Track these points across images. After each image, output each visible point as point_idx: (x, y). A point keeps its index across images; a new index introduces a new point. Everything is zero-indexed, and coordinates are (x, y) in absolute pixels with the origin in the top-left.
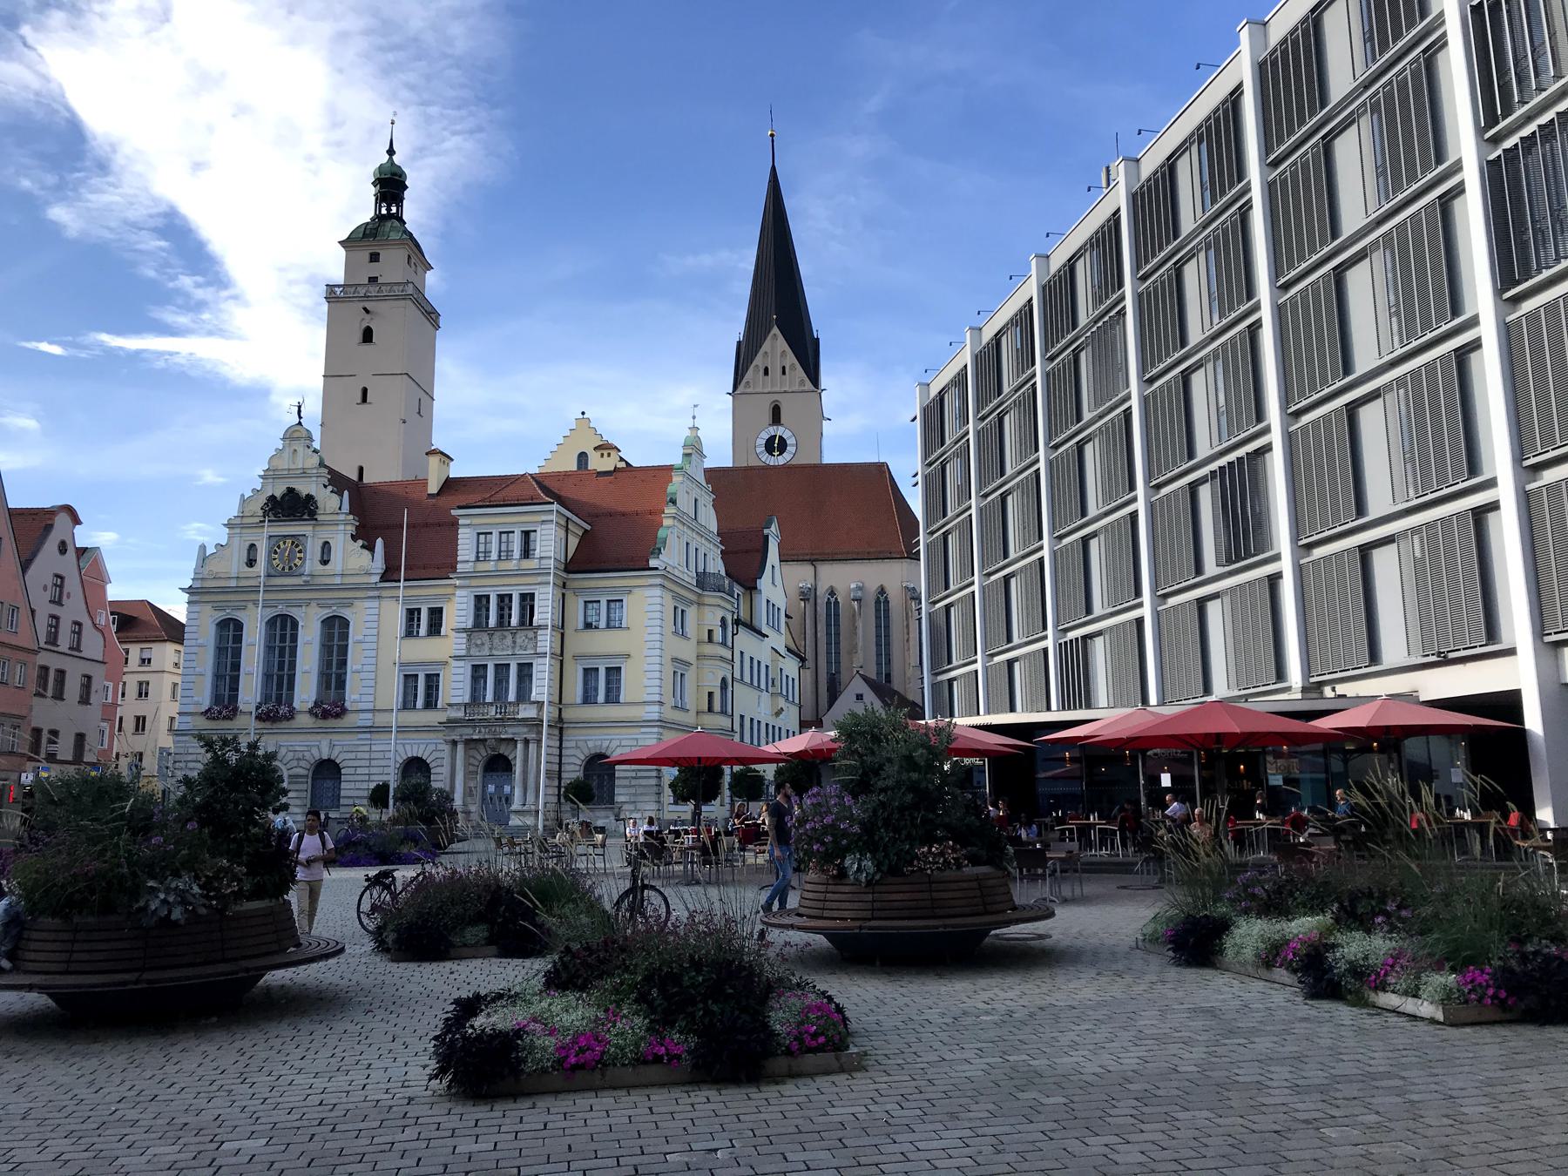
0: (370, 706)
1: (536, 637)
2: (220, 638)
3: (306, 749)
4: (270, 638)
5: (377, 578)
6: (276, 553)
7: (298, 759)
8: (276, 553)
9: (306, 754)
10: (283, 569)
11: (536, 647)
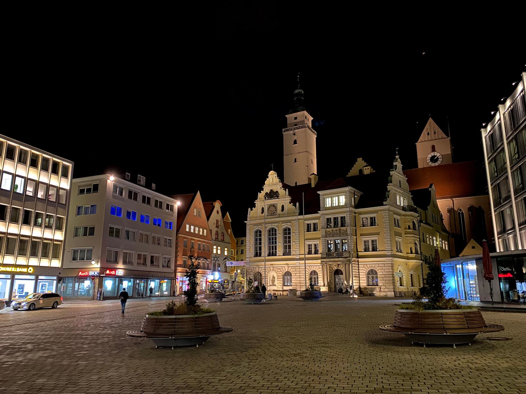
2: (256, 236)
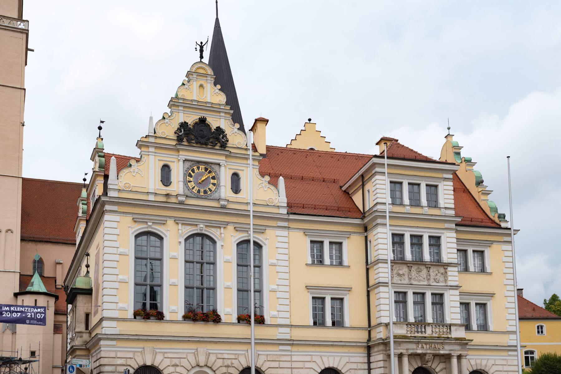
0: (287, 322)
1: (446, 272)
3: (233, 357)
5: (284, 211)
7: (228, 366)
8: (190, 176)
10: (199, 191)
11: (446, 281)
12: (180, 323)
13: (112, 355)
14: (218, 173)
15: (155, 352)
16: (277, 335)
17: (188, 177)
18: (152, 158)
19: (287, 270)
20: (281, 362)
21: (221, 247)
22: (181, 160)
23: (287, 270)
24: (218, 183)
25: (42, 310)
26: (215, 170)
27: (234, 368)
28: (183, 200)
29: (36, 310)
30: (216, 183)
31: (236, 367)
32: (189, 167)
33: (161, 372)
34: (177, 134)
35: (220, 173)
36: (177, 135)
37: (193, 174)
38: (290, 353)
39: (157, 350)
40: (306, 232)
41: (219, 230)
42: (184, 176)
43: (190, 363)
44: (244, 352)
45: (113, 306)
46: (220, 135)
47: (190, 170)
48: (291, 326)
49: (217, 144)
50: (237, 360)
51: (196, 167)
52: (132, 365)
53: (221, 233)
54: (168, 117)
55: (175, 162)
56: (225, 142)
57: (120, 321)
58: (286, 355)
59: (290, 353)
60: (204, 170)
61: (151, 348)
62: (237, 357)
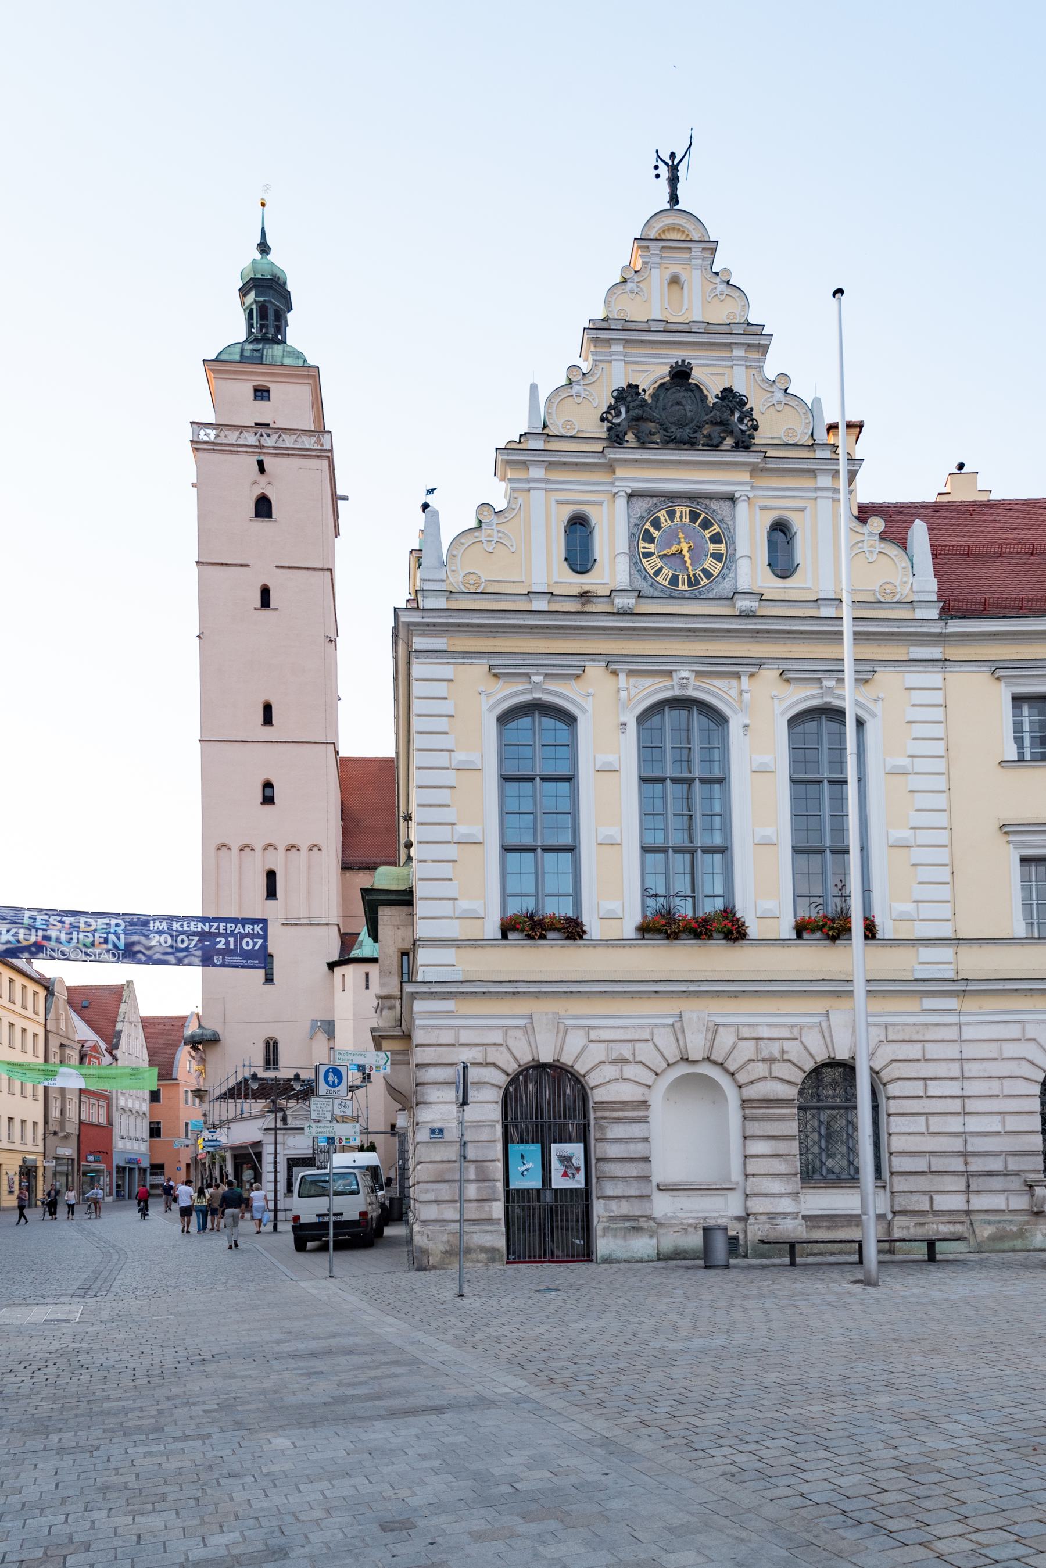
0: (945, 931)
3: (785, 1033)
4: (648, 750)
6: (651, 539)
7: (772, 1060)
8: (649, 538)
9: (788, 1045)
10: (674, 580)
12: (631, 946)
13: (447, 1037)
14: (730, 523)
15: (561, 1026)
16: (913, 970)
17: (641, 542)
18: (537, 497)
19: (941, 783)
20: (927, 1045)
21: (741, 730)
22: (621, 494)
23: (941, 783)
24: (729, 552)
25: (257, 929)
26: (719, 517)
27: (789, 1064)
28: (630, 606)
29: (239, 929)
30: (723, 551)
31: (795, 1061)
32: (645, 514)
33: (582, 1079)
34: (609, 422)
35: (734, 522)
36: (606, 424)
37: (656, 534)
38: (954, 1019)
39: (570, 1022)
40: (997, 669)
41: (734, 682)
42: (630, 541)
43: (662, 1053)
44: (817, 1020)
45: (445, 909)
46: (732, 413)
47: (648, 523)
48: (957, 942)
49: (724, 439)
50: (797, 1042)
51: (664, 512)
52: (500, 1065)
53: (741, 692)
54: (580, 377)
55: (605, 504)
56: (748, 433)
57: (466, 946)
58: (945, 1024)
59: (954, 1019)
60: (688, 520)
61: (550, 1016)
62: (796, 1032)
